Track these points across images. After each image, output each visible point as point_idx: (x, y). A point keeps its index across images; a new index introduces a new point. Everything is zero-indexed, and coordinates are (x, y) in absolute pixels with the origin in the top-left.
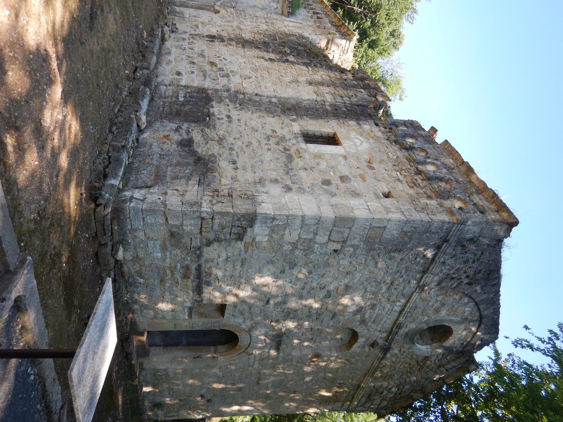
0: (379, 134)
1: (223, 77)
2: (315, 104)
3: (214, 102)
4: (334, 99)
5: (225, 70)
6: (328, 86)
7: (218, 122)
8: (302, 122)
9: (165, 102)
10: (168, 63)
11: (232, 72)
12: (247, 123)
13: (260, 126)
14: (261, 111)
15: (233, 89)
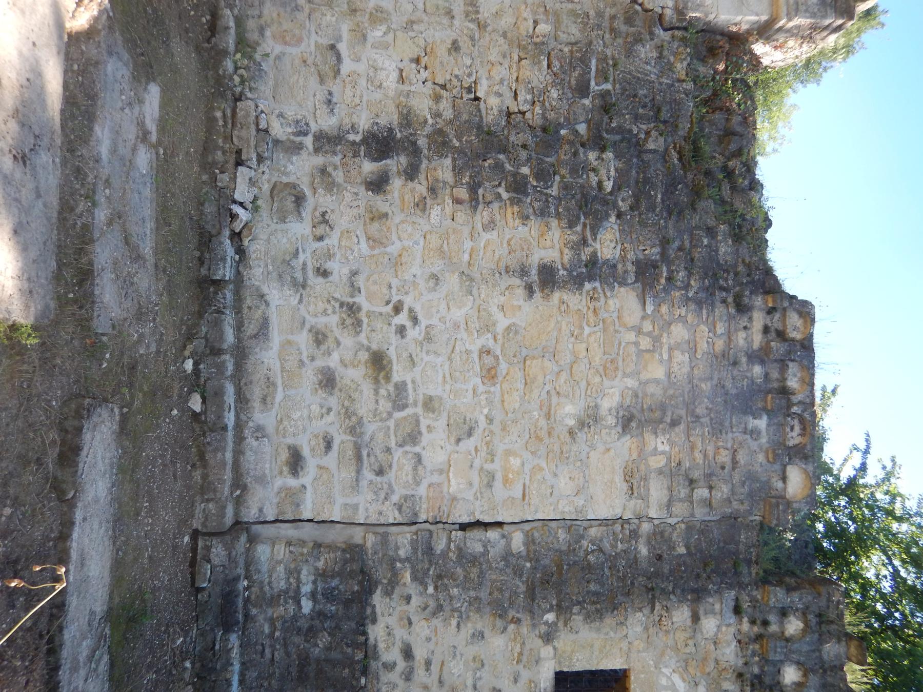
0: (730, 653)
1: (400, 446)
2: (616, 539)
3: (379, 591)
4: (669, 504)
5: (411, 400)
6: (674, 423)
7: (386, 677)
8: (564, 641)
9: (272, 621)
10: (264, 400)
11: (429, 404)
12: (445, 676)
13: (469, 682)
14: (478, 610)
15: (423, 517)
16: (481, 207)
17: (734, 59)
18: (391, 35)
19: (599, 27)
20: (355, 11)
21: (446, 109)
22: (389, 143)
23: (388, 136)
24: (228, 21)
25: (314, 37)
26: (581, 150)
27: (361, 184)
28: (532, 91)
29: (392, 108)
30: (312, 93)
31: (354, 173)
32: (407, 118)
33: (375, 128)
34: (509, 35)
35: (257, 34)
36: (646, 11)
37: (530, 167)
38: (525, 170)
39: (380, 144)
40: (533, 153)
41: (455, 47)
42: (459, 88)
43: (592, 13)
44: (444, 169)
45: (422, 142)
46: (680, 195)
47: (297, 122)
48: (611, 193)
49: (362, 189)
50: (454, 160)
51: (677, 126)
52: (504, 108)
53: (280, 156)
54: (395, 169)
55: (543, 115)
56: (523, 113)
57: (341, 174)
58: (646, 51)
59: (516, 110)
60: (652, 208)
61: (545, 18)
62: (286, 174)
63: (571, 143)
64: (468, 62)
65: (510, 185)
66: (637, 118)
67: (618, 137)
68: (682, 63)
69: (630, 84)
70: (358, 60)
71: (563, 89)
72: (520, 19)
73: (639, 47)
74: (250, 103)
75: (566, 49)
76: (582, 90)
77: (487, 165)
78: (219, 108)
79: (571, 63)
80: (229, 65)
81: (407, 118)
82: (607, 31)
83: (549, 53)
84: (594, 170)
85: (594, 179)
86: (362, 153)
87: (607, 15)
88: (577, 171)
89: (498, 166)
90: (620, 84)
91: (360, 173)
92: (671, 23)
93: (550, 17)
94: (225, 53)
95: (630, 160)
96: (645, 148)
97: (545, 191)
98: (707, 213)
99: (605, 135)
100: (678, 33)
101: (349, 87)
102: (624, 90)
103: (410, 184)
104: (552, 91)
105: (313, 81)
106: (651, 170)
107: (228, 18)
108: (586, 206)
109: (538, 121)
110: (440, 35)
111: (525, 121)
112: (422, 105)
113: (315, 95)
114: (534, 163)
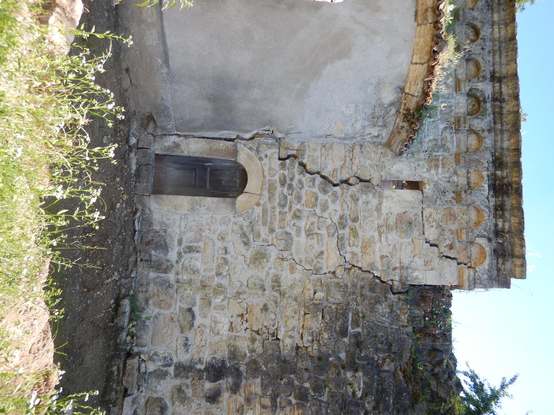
16: (278, 410)
17: (437, 302)
18: (226, 301)
19: (354, 293)
20: (205, 286)
21: (258, 346)
22: (222, 371)
23: (221, 366)
24: (125, 309)
25: (179, 303)
26: (342, 371)
27: (203, 397)
28: (312, 334)
29: (225, 347)
30: (176, 338)
31: (199, 390)
32: (234, 354)
33: (214, 361)
34: (298, 299)
35: (144, 303)
36: (382, 282)
37: (310, 383)
38: (307, 385)
39: (216, 371)
40: (312, 375)
41: (265, 308)
42: (266, 334)
43: (349, 285)
44: (255, 385)
45: (243, 368)
46: (404, 400)
47: (165, 358)
48: (361, 398)
49: (204, 401)
50: (262, 380)
51: (402, 356)
52: (295, 345)
53: (153, 381)
54: (225, 386)
55: (319, 351)
56: (307, 347)
57: (191, 391)
58: (383, 308)
59: (302, 346)
60: (387, 408)
61: (321, 288)
62: (155, 392)
63: (336, 366)
64: (273, 317)
65: (297, 396)
66: (377, 350)
67: (365, 362)
68: (405, 315)
69: (372, 329)
70: (205, 317)
71: (331, 332)
72: (305, 289)
73: (378, 306)
74: (136, 360)
75: (333, 307)
76: (343, 333)
77: (283, 383)
78: (115, 365)
79: (336, 316)
80: (124, 334)
81: (234, 354)
82: (359, 295)
83: (323, 309)
84: (350, 384)
85: (350, 391)
86: (205, 377)
87: (359, 285)
88: (339, 386)
89: (290, 383)
90: (367, 329)
91: (202, 390)
92: (398, 290)
93: (324, 288)
94: (122, 329)
95: (373, 377)
96: (382, 369)
97: (319, 398)
98: (422, 411)
99: (357, 361)
100: (402, 297)
101: (199, 334)
102: (369, 333)
103: (234, 396)
104: (325, 334)
105: (177, 331)
106: (386, 383)
107: (126, 303)
108: (345, 408)
109: (315, 353)
110: (256, 301)
111: (308, 353)
112: (244, 345)
113: (177, 340)
114: (313, 381)
